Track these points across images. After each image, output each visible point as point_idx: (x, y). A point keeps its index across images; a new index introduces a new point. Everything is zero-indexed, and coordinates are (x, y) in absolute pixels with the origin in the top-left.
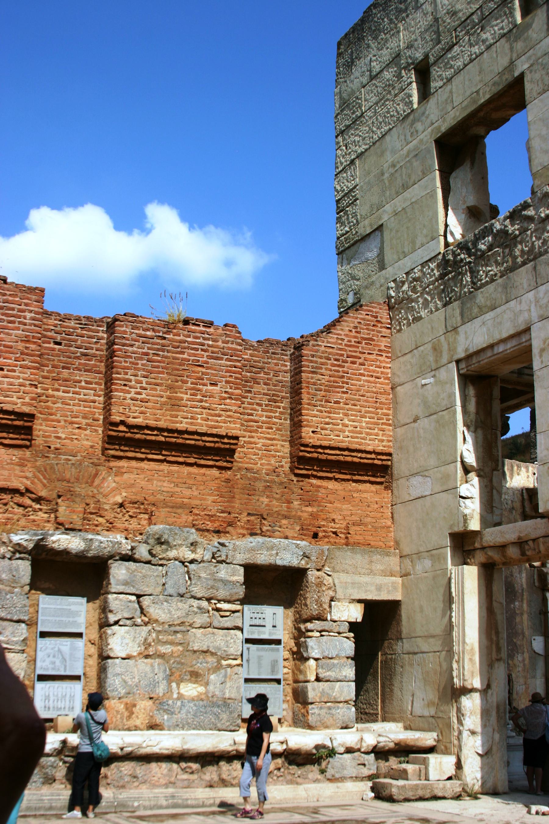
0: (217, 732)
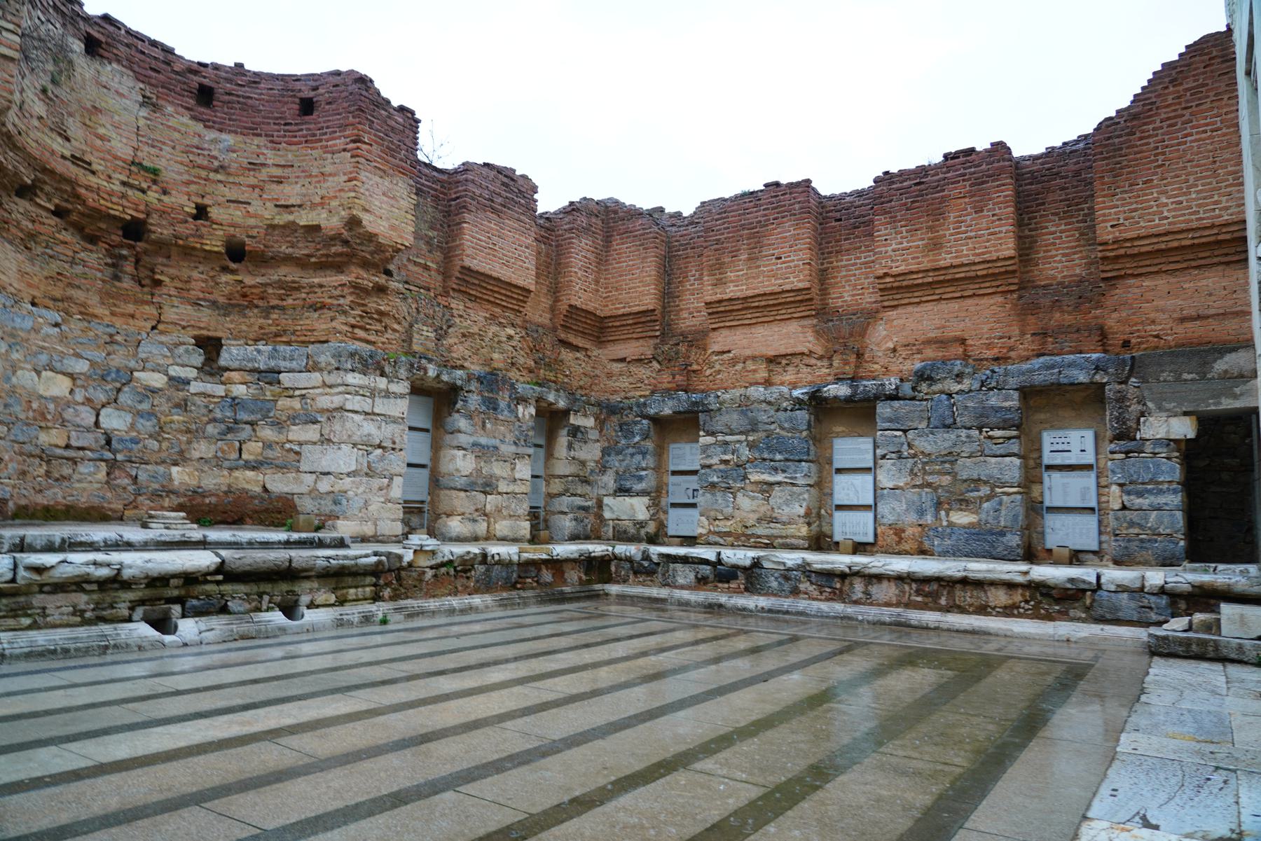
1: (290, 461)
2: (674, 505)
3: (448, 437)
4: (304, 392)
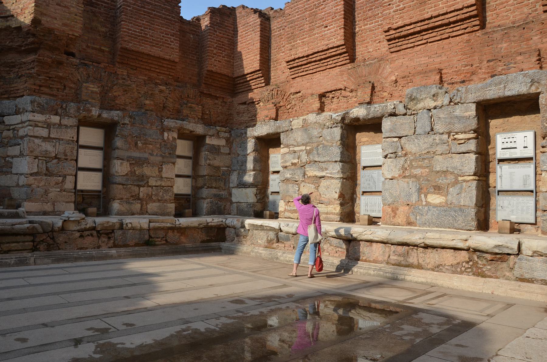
0: (455, 230)
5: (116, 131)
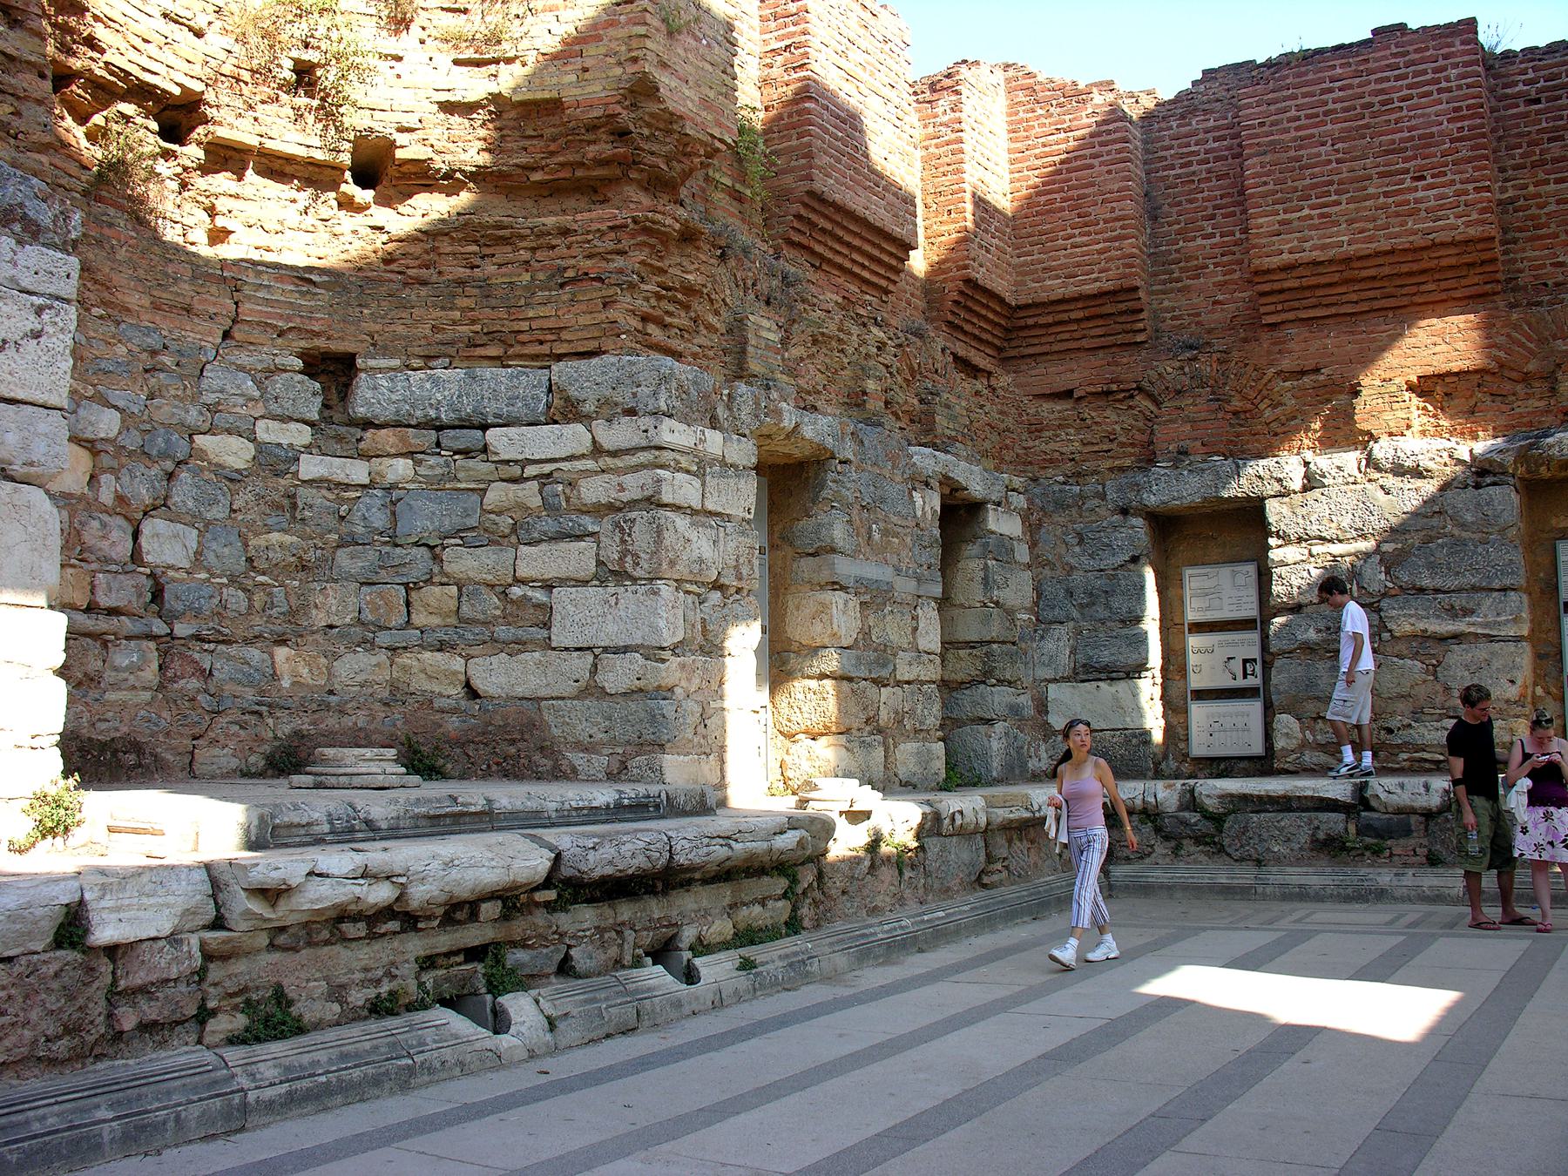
1: (525, 619)
2: (1200, 695)
3: (806, 564)
4: (547, 468)
5: (822, 486)
